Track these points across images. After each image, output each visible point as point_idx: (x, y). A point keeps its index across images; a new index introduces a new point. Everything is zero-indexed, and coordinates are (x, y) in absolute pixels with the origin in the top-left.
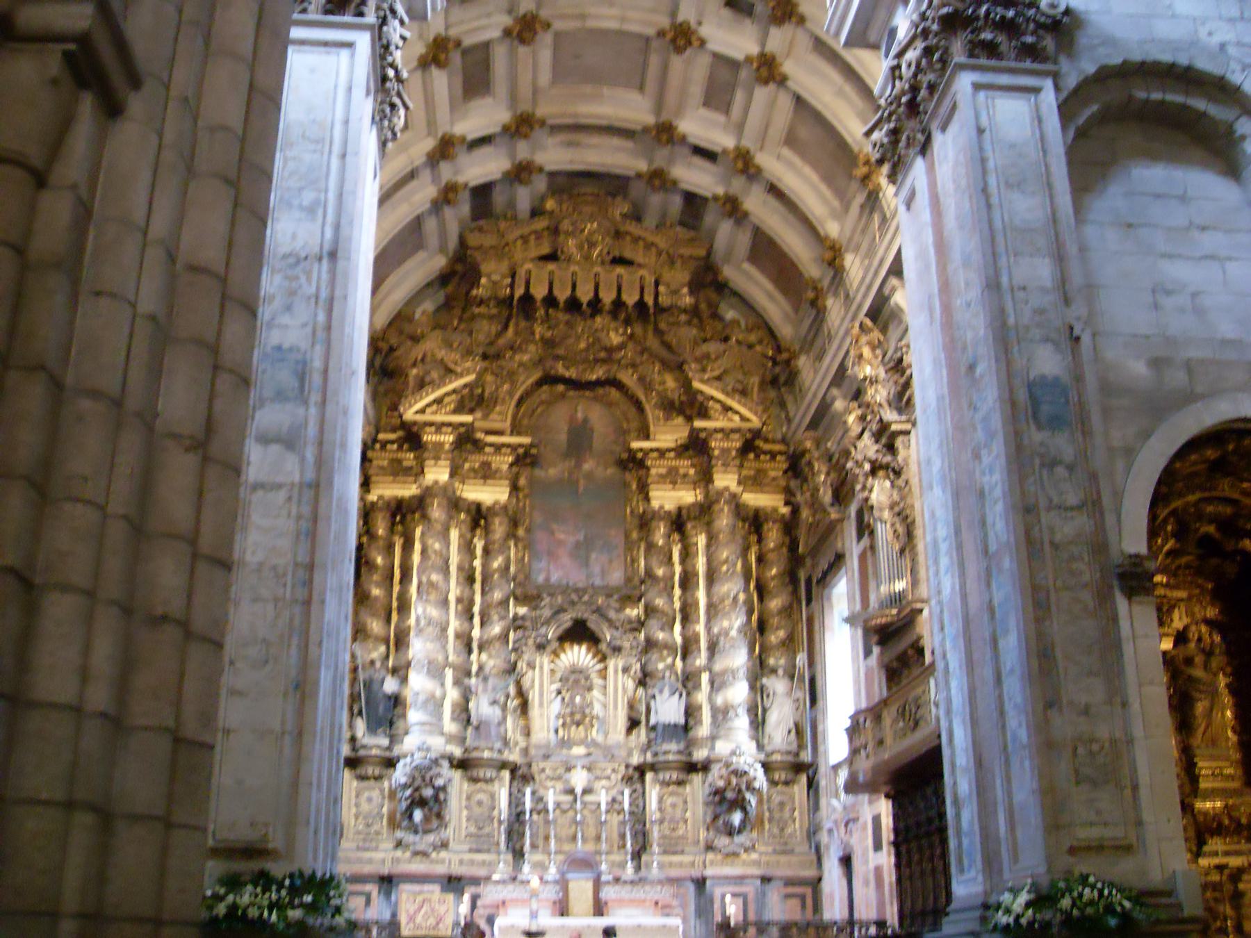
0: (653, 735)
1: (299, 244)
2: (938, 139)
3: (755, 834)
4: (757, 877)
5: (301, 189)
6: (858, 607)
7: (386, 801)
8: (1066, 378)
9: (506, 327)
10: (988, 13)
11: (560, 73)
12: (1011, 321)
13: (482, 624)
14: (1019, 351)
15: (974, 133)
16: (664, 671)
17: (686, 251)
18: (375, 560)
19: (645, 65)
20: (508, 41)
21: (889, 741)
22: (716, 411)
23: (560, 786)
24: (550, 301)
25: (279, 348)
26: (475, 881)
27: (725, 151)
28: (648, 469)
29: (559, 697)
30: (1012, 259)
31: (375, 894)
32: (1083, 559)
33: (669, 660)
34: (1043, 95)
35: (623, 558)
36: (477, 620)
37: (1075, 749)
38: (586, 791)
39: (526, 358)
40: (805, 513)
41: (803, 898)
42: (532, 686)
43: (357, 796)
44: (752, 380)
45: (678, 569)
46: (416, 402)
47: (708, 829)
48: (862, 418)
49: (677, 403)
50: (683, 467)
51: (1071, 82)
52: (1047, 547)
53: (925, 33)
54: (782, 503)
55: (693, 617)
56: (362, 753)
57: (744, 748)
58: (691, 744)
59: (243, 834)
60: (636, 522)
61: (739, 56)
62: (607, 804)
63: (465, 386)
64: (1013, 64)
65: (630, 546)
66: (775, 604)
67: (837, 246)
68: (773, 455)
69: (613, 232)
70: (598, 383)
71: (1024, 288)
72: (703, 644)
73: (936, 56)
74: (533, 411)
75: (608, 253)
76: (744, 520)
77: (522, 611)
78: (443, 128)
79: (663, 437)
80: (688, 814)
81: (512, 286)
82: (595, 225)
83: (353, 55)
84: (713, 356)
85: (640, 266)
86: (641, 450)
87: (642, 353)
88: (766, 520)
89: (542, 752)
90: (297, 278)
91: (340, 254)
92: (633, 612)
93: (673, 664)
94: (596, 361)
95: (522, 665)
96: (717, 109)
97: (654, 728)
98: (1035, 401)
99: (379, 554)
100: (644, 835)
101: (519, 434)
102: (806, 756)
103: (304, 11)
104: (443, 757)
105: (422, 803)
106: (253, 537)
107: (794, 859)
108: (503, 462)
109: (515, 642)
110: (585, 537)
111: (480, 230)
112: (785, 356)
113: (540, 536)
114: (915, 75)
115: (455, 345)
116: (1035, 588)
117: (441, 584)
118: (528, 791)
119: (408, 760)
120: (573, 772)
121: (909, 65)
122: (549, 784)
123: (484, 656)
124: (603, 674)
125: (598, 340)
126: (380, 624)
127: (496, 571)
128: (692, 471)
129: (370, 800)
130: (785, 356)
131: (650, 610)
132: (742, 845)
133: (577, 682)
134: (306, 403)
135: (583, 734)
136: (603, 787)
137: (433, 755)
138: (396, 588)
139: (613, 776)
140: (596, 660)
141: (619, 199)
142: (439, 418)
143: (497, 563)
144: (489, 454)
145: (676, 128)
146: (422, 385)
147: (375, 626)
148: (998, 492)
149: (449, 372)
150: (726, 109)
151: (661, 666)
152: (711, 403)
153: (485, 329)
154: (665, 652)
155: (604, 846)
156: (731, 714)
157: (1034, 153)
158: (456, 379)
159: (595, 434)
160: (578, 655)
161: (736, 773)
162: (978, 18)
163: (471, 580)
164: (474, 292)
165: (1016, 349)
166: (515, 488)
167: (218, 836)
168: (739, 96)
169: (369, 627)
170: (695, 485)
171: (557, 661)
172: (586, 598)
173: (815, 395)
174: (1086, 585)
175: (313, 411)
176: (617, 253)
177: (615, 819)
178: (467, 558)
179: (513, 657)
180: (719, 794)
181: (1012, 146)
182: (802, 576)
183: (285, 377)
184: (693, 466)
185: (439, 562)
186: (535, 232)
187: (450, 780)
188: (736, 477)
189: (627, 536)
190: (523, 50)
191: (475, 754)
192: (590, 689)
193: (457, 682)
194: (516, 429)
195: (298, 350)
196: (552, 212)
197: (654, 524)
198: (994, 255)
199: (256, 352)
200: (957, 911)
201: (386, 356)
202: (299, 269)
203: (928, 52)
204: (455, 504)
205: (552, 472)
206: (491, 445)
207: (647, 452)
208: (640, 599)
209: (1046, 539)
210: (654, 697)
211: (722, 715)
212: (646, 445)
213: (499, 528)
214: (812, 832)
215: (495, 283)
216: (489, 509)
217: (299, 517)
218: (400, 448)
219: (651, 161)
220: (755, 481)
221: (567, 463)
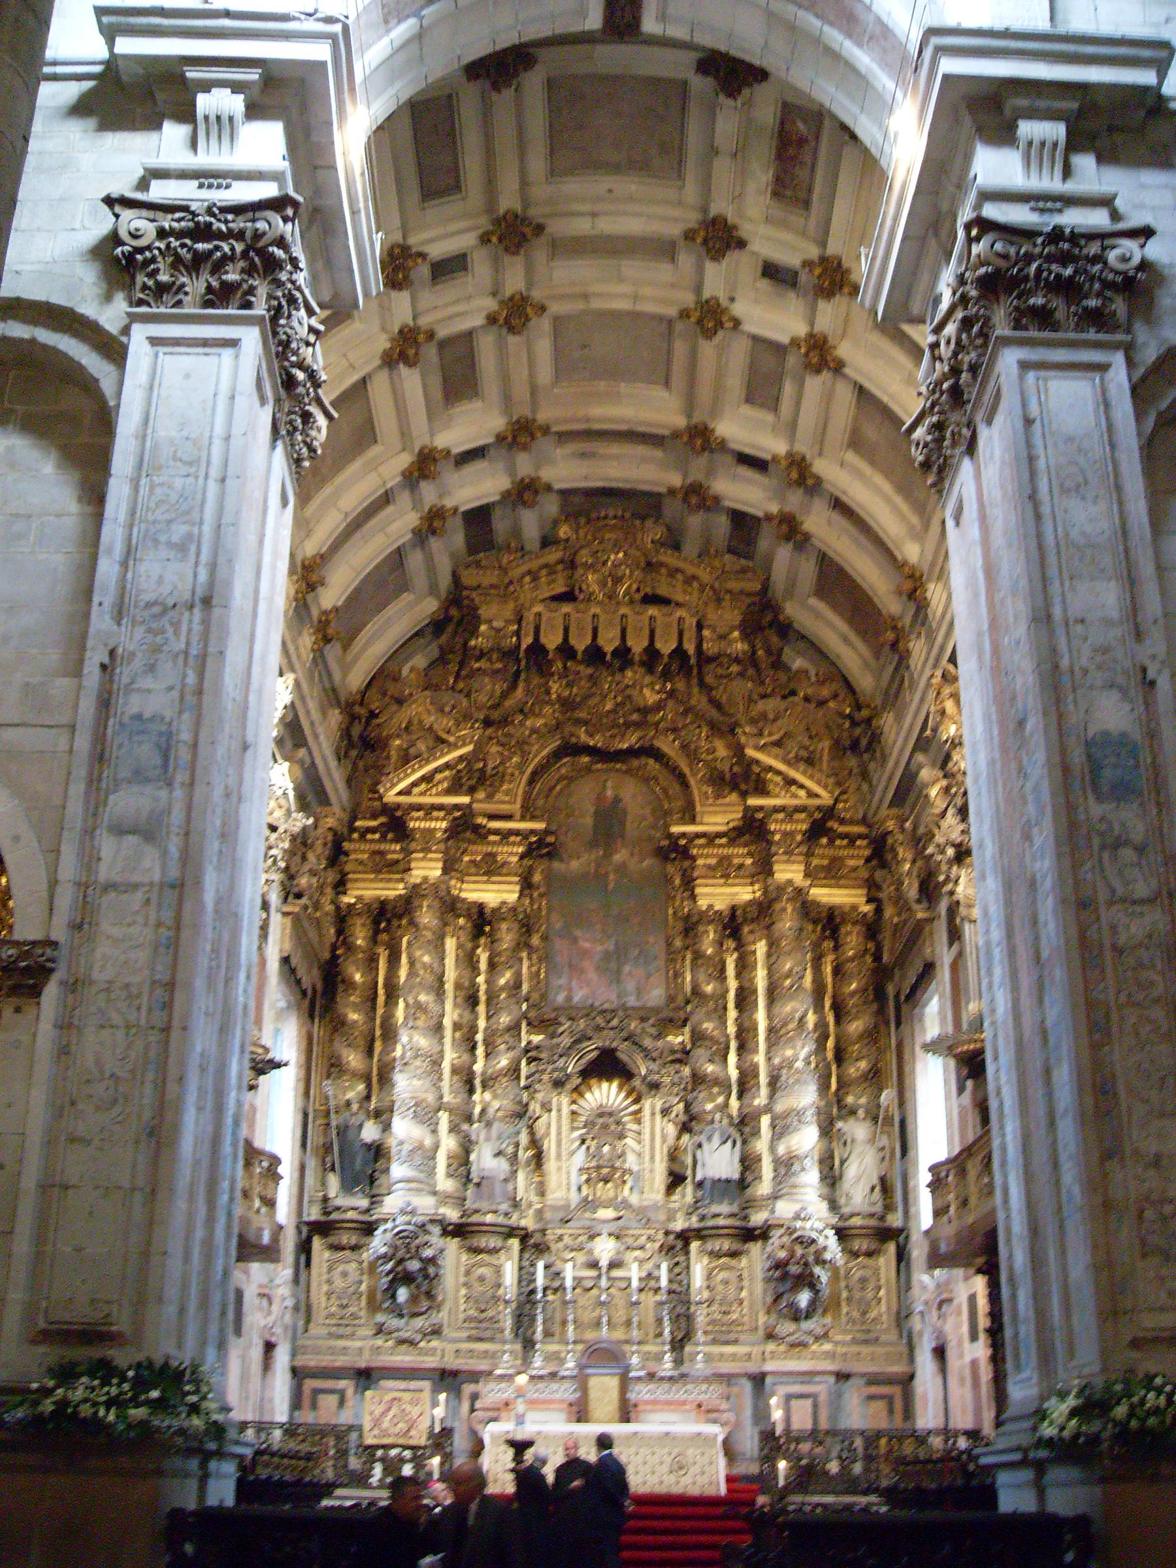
0: (700, 1194)
1: (166, 589)
2: (983, 433)
3: (828, 1320)
5: (170, 522)
6: (950, 1029)
7: (365, 1277)
8: (1137, 735)
9: (514, 686)
10: (1039, 271)
11: (563, 368)
12: (1065, 663)
13: (487, 1055)
14: (1075, 701)
15: (1019, 424)
16: (712, 1112)
17: (734, 585)
18: (352, 977)
19: (669, 352)
20: (495, 328)
21: (973, 1200)
22: (777, 784)
23: (581, 1258)
24: (566, 650)
25: (138, 717)
26: (475, 1376)
27: (775, 458)
28: (694, 859)
30: (1067, 584)
31: (350, 1392)
32: (1154, 967)
33: (720, 1100)
34: (1111, 373)
35: (663, 972)
36: (480, 1051)
37: (1141, 1211)
38: (613, 1265)
39: (539, 722)
40: (889, 912)
41: (890, 1399)
42: (548, 1134)
43: (330, 1270)
44: (820, 746)
45: (732, 984)
46: (400, 780)
48: (947, 790)
49: (728, 776)
50: (738, 856)
51: (1150, 354)
52: (1108, 955)
53: (964, 300)
54: (864, 899)
55: (750, 1045)
56: (335, 1216)
57: (810, 1210)
58: (748, 1205)
59: (81, 1313)
60: (680, 926)
61: (785, 339)
62: (640, 1279)
63: (461, 758)
64: (1072, 335)
65: (672, 956)
66: (855, 1027)
67: (918, 574)
68: (852, 839)
69: (643, 564)
70: (631, 753)
71: (1083, 621)
72: (763, 1079)
73: (975, 329)
74: (551, 789)
75: (638, 590)
76: (815, 922)
77: (537, 1039)
78: (421, 438)
79: (713, 819)
80: (744, 1294)
81: (517, 633)
82: (621, 555)
83: (237, 357)
84: (771, 716)
85: (678, 605)
86: (684, 835)
87: (686, 713)
88: (843, 921)
89: (561, 1215)
90: (163, 632)
91: (215, 601)
92: (676, 1039)
93: (726, 1105)
94: (627, 725)
95: (535, 1108)
96: (762, 406)
97: (700, 1185)
98: (1094, 767)
101: (533, 818)
102: (895, 1220)
103: (179, 303)
104: (432, 1221)
105: (407, 1278)
106: (103, 949)
107: (880, 1350)
108: (511, 853)
109: (527, 1078)
110: (616, 944)
111: (478, 564)
112: (865, 713)
113: (560, 945)
114: (955, 354)
115: (447, 709)
116: (1091, 1005)
117: (434, 1008)
118: (540, 1265)
119: (389, 1225)
120: (597, 1239)
121: (948, 342)
123: (487, 1096)
124: (637, 1116)
125: (629, 697)
126: (359, 1056)
127: (502, 989)
128: (749, 861)
129: (345, 1274)
130: (865, 713)
131: (698, 1037)
132: (810, 1333)
133: (605, 1126)
134: (170, 784)
136: (636, 1259)
137: (419, 1219)
138: (380, 1011)
139: (648, 1245)
141: (649, 523)
142: (427, 800)
144: (494, 843)
145: (713, 430)
146: (406, 759)
147: (353, 1059)
148: (1048, 883)
150: (774, 405)
151: (709, 1106)
153: (487, 689)
155: (635, 1334)
156: (796, 1167)
157: (1098, 449)
158: (448, 753)
159: (629, 817)
161: (800, 1240)
162: (1026, 278)
164: (473, 643)
165: (1070, 699)
166: (527, 885)
167: (52, 1317)
168: (788, 388)
170: (753, 878)
171: (581, 1102)
172: (615, 1022)
173: (897, 763)
174: (1156, 1001)
175: (179, 793)
176: (648, 590)
177: (650, 1299)
178: (467, 974)
179: (525, 1096)
180: (779, 1265)
181: (1070, 440)
182: (891, 990)
183: (146, 752)
184: (750, 854)
185: (430, 978)
186: (546, 566)
187: (442, 1251)
188: (802, 867)
189: (669, 944)
190: (513, 340)
191: (475, 1218)
192: (622, 1136)
193: (454, 1129)
194: (528, 812)
195: (163, 718)
196: (567, 540)
197: (701, 928)
198: (1044, 580)
199: (111, 722)
200: (1014, 1419)
201: (368, 723)
202: (165, 621)
203: (967, 323)
204: (451, 906)
205: (575, 864)
206: (496, 832)
208: (685, 1022)
209: (1107, 945)
210: (700, 1146)
211: (786, 1166)
213: (507, 936)
214: (902, 1317)
215: (499, 630)
216: (495, 911)
217: (159, 924)
218: (384, 837)
219: (685, 475)
220: (831, 873)
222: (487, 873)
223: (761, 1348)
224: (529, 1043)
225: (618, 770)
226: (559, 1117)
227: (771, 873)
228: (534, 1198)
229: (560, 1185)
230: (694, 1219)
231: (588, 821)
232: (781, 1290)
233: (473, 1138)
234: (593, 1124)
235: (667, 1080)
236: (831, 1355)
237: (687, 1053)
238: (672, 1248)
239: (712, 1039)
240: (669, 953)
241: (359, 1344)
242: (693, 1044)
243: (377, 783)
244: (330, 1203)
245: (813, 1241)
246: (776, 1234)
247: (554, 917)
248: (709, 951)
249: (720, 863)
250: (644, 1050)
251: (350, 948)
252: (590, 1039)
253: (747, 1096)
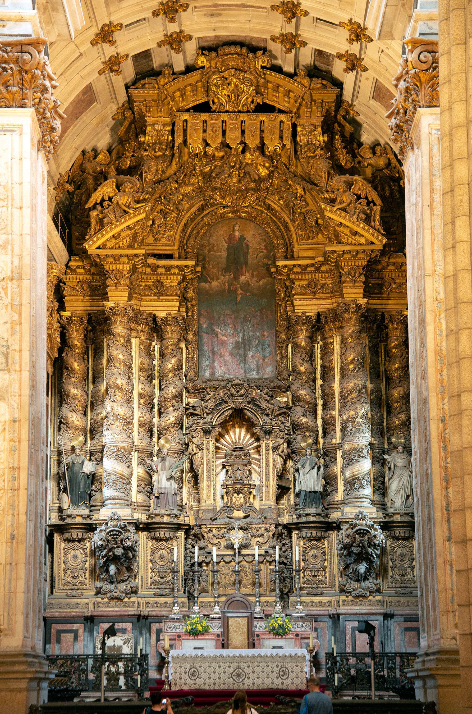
4: (380, 614)
13: (160, 414)
18: (72, 365)
26: (159, 619)
29: (225, 470)
31: (81, 631)
33: (310, 441)
35: (274, 355)
36: (156, 409)
42: (202, 464)
45: (319, 362)
46: (98, 239)
47: (341, 576)
55: (329, 405)
56: (68, 521)
58: (329, 507)
62: (260, 555)
74: (198, 232)
77: (193, 401)
80: (326, 564)
86: (286, 266)
92: (283, 400)
93: (316, 442)
94: (247, 190)
99: (75, 361)
100: (292, 578)
101: (186, 258)
105: (115, 559)
110: (243, 338)
113: (206, 338)
119: (103, 527)
120: (232, 532)
122: (216, 541)
123: (162, 441)
129: (75, 557)
131: (296, 399)
132: (367, 589)
135: (242, 500)
137: (122, 523)
139: (265, 534)
140: (253, 439)
143: (171, 363)
151: (303, 445)
152: (341, 229)
154: (307, 434)
156: (357, 485)
158: (130, 219)
159: (250, 250)
161: (359, 532)
163: (150, 378)
166: (184, 299)
169: (70, 421)
171: (222, 441)
172: (242, 392)
177: (266, 569)
178: (146, 361)
180: (346, 547)
188: (362, 291)
189: (277, 337)
191: (157, 520)
192: (248, 463)
205: (214, 283)
206: (164, 267)
208: (288, 388)
210: (297, 470)
221: (227, 277)
222: (158, 294)
223: (337, 598)
224: (188, 403)
225: (243, 218)
226: (208, 453)
227: (342, 295)
228: (195, 504)
229: (209, 497)
230: (295, 516)
231: (224, 254)
232: (349, 562)
233: (154, 468)
234: (230, 456)
235: (276, 429)
236: (382, 603)
237: (290, 409)
238: (281, 535)
239: (305, 401)
240: (276, 342)
241: (86, 601)
242: (293, 403)
243: (84, 239)
244: (64, 513)
245: (368, 532)
246: (344, 527)
247: (203, 320)
248: (303, 344)
249: (309, 285)
250: (261, 409)
251: (71, 347)
252: (226, 403)
253: (329, 437)
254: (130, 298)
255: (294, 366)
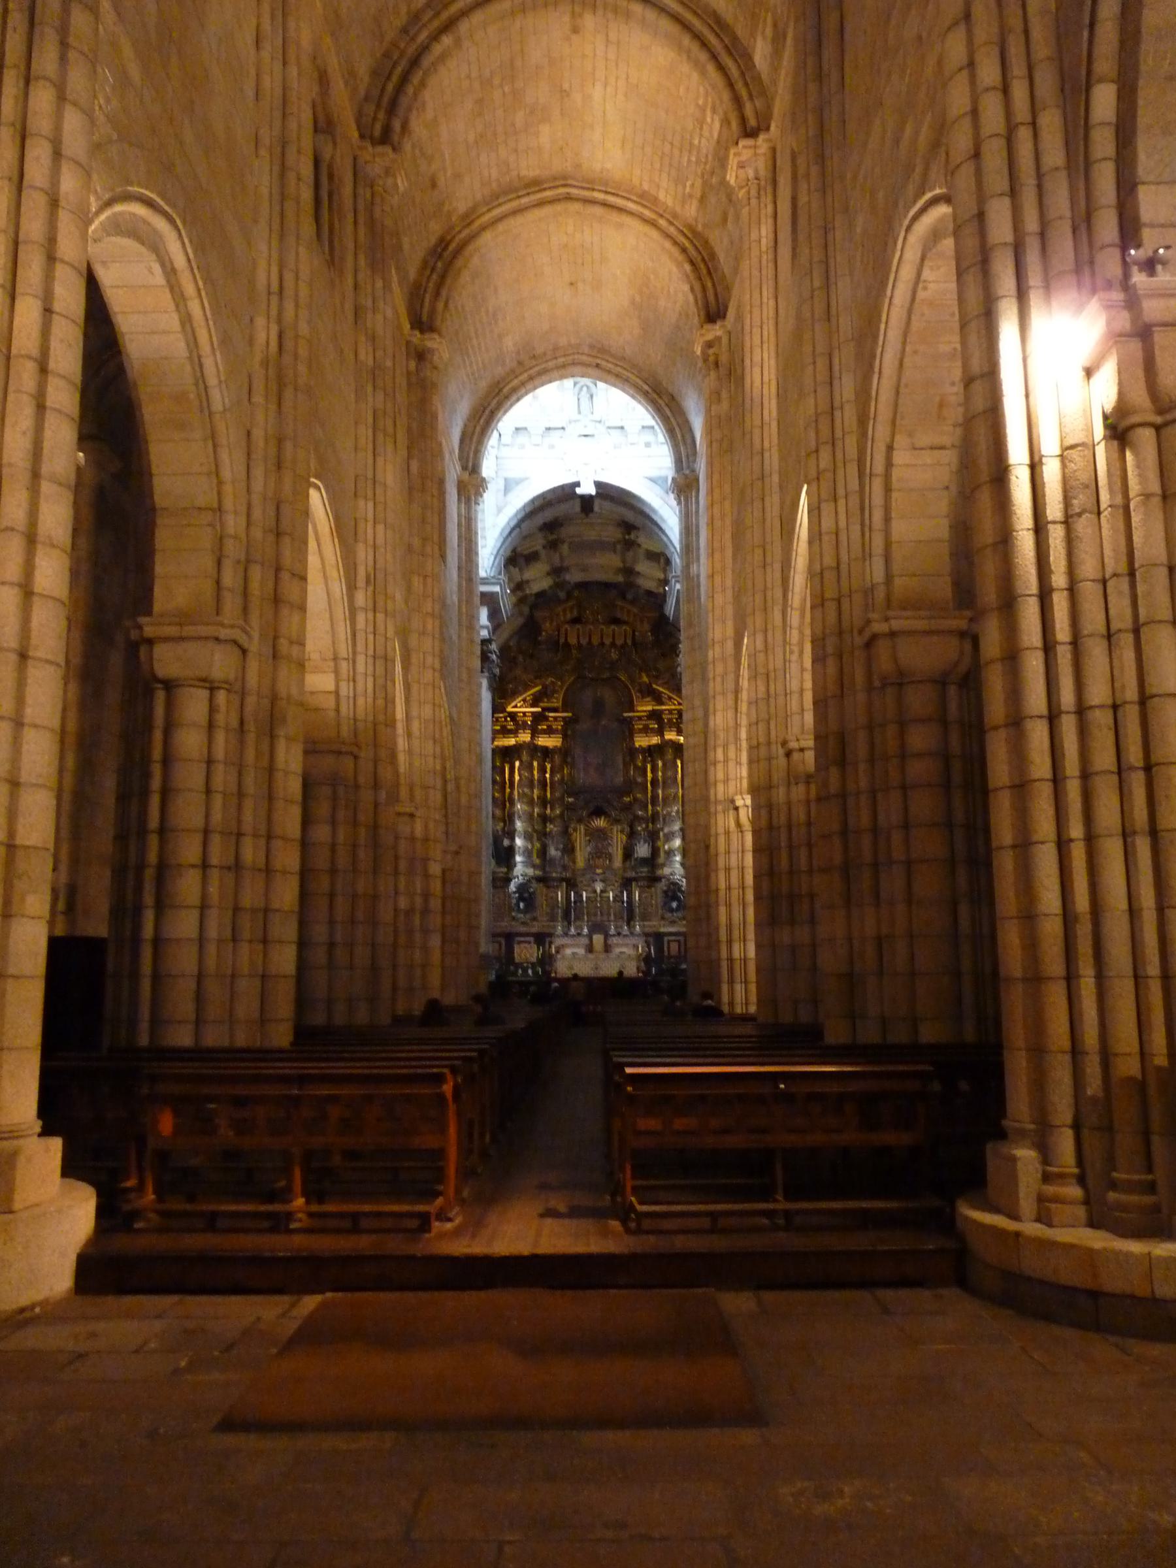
45: (649, 775)
77: (570, 800)
92: (627, 799)
93: (647, 827)
95: (571, 830)
101: (567, 711)
108: (558, 726)
131: (635, 799)
138: (508, 790)
143: (558, 777)
149: (527, 688)
160: (601, 823)
163: (543, 784)
193: (539, 839)
204: (534, 749)
207: (631, 718)
212: (631, 714)
227: (662, 736)
254: (533, 737)
255: (635, 779)
